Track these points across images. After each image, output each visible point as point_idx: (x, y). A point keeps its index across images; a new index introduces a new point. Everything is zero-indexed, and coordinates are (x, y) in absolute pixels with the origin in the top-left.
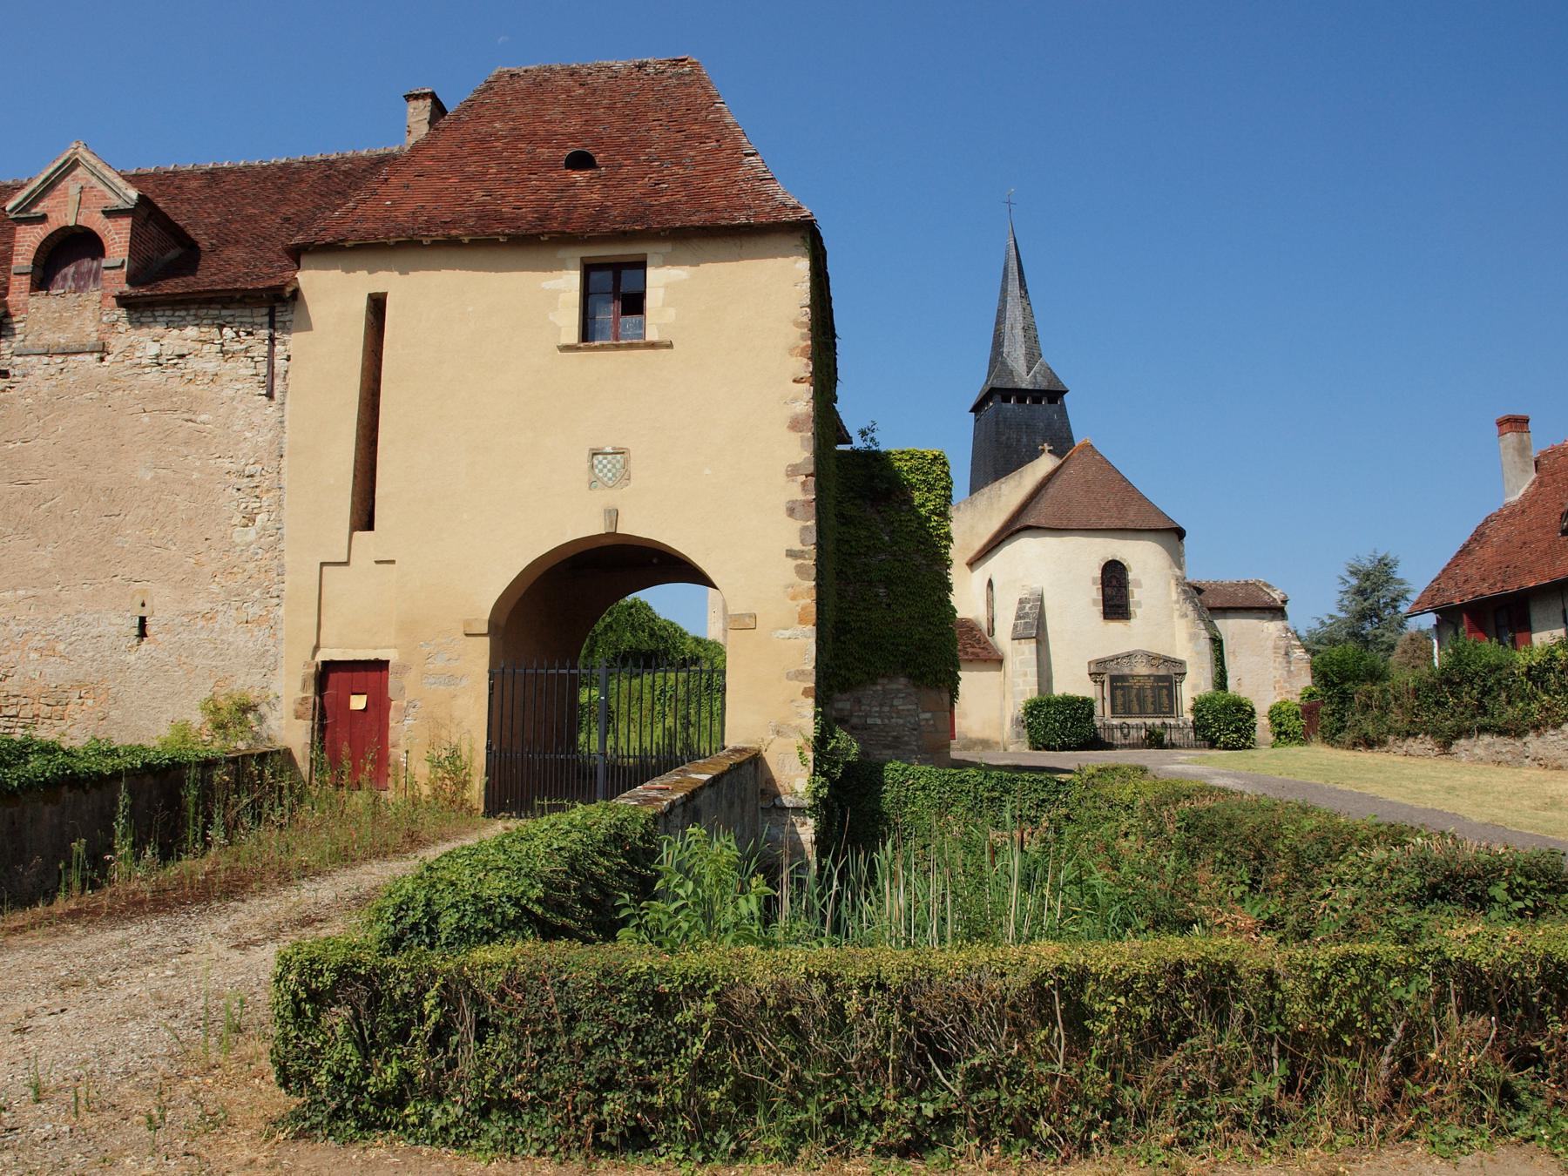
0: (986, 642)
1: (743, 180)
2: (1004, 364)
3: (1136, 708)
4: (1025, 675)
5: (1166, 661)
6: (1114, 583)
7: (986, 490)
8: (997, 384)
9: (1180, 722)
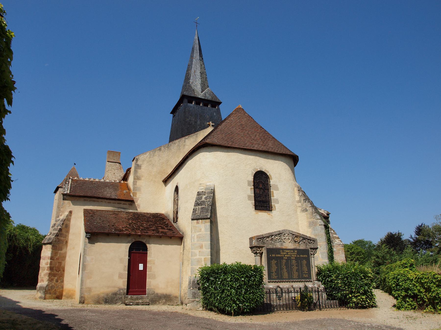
0: (172, 226)
2: (190, 86)
3: (286, 275)
4: (201, 247)
5: (304, 239)
6: (261, 186)
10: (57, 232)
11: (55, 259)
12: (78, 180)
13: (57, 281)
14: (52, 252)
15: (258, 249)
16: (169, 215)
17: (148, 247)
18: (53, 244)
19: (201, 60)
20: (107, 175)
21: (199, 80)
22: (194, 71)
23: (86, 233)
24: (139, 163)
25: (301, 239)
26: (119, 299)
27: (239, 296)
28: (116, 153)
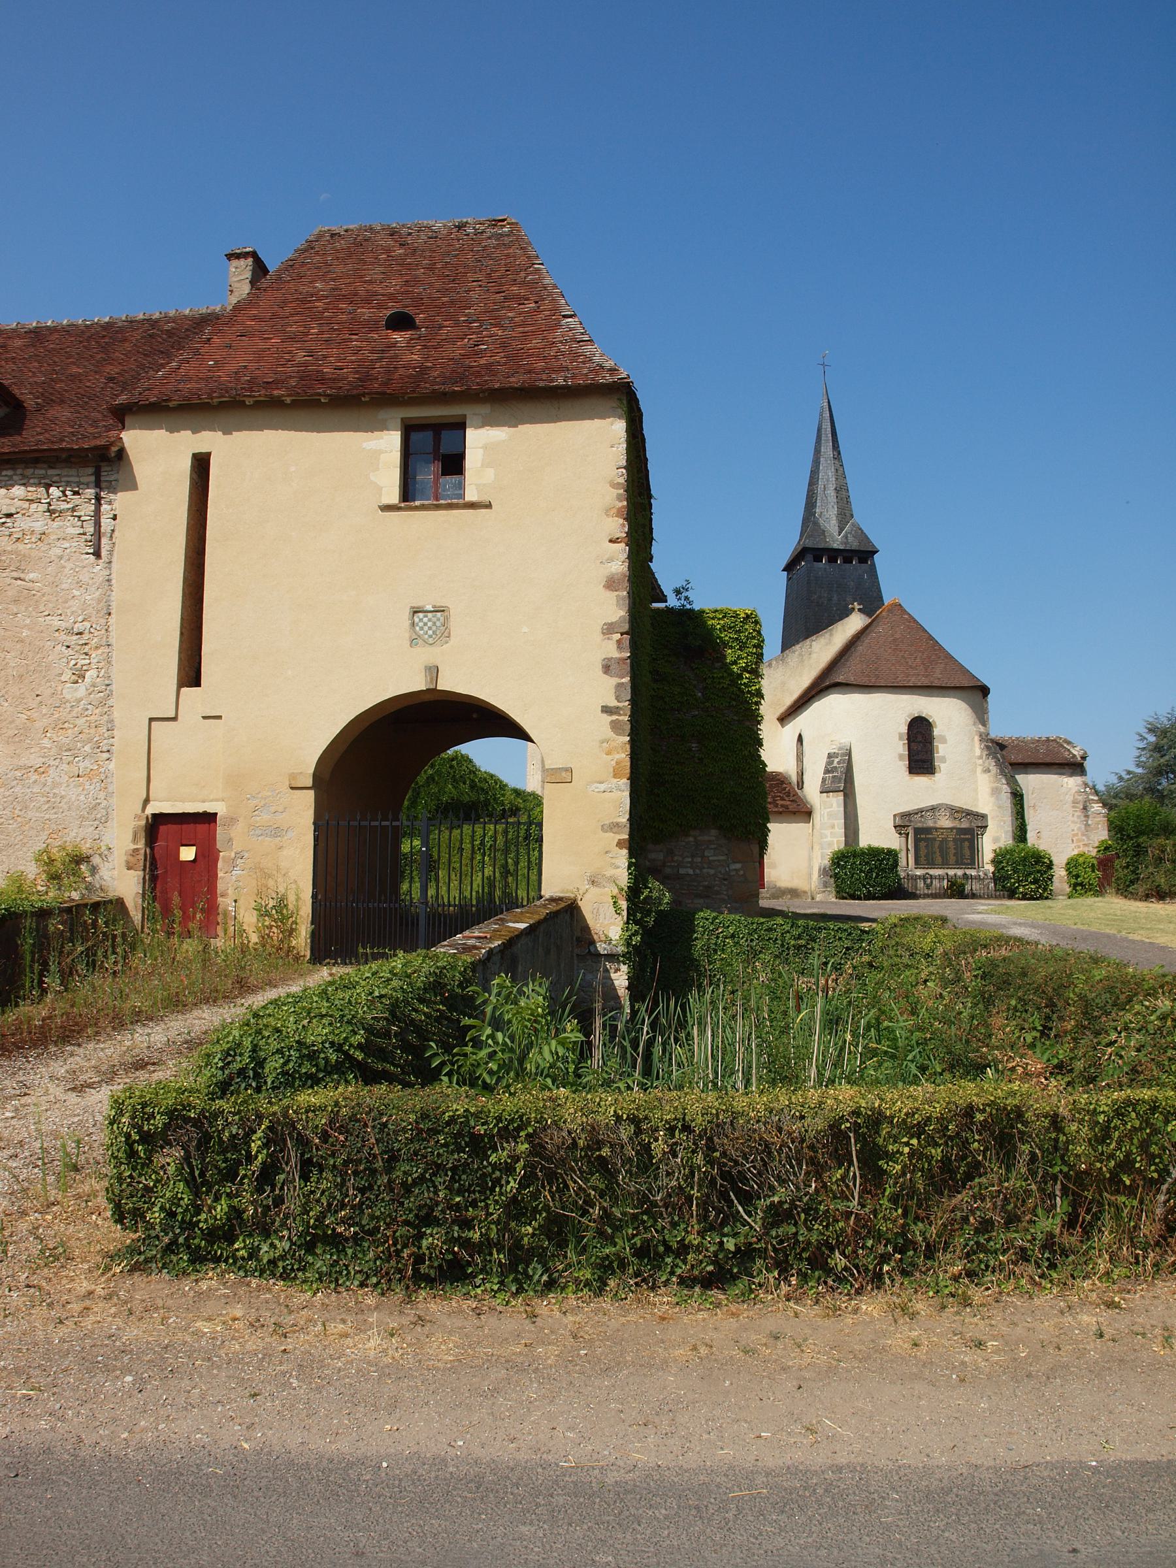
0: (796, 794)
1: (561, 342)
2: (816, 524)
3: (939, 860)
4: (833, 827)
5: (968, 814)
6: (920, 738)
7: (797, 647)
8: (810, 544)
9: (981, 873)
16: (790, 776)
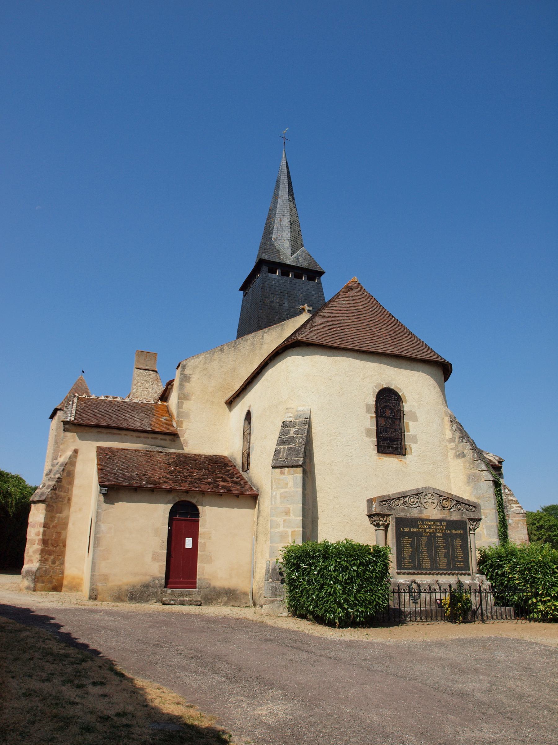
0: (240, 477)
2: (272, 245)
3: (426, 562)
4: (287, 513)
6: (388, 414)
7: (250, 336)
10: (54, 483)
11: (51, 526)
12: (88, 399)
13: (54, 562)
14: (46, 514)
15: (381, 519)
16: (235, 459)
17: (200, 511)
18: (47, 503)
19: (291, 200)
20: (135, 390)
21: (287, 235)
22: (279, 219)
23: (101, 486)
24: (187, 372)
25: (454, 503)
26: (153, 594)
27: (349, 595)
28: (150, 354)
